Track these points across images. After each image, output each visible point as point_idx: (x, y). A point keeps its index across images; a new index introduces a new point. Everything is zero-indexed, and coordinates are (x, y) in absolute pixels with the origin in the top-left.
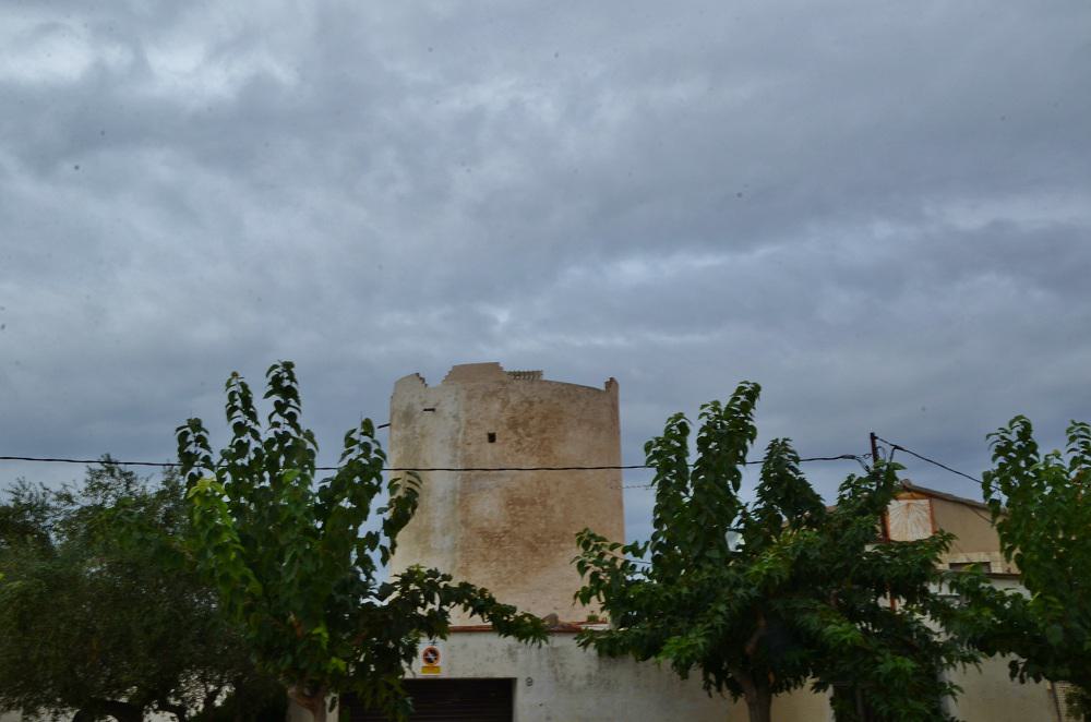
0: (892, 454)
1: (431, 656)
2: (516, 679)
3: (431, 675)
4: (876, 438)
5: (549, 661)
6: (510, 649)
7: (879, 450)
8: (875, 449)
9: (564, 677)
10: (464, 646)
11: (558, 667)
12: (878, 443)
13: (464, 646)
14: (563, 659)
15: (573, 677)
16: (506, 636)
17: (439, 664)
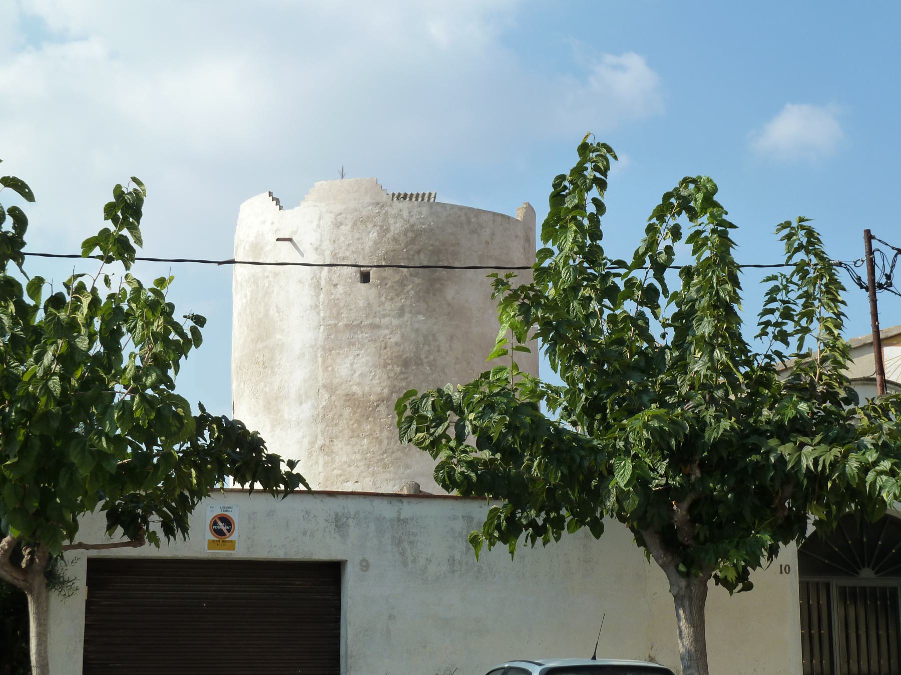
0: (894, 261)
1: (221, 526)
2: (347, 561)
3: (222, 554)
4: (874, 238)
5: (393, 537)
6: (337, 519)
7: (877, 254)
8: (870, 252)
9: (414, 561)
10: (271, 513)
11: (406, 545)
12: (875, 244)
13: (271, 513)
14: (414, 535)
15: (429, 560)
16: (2, 228)
17: (233, 537)
